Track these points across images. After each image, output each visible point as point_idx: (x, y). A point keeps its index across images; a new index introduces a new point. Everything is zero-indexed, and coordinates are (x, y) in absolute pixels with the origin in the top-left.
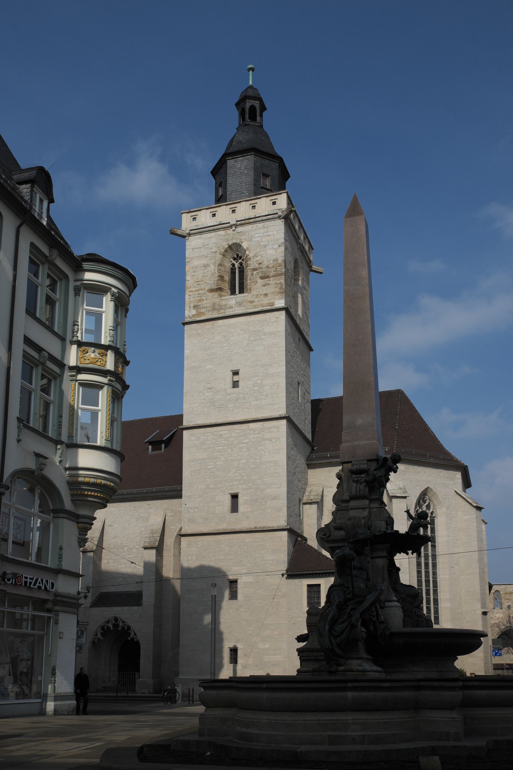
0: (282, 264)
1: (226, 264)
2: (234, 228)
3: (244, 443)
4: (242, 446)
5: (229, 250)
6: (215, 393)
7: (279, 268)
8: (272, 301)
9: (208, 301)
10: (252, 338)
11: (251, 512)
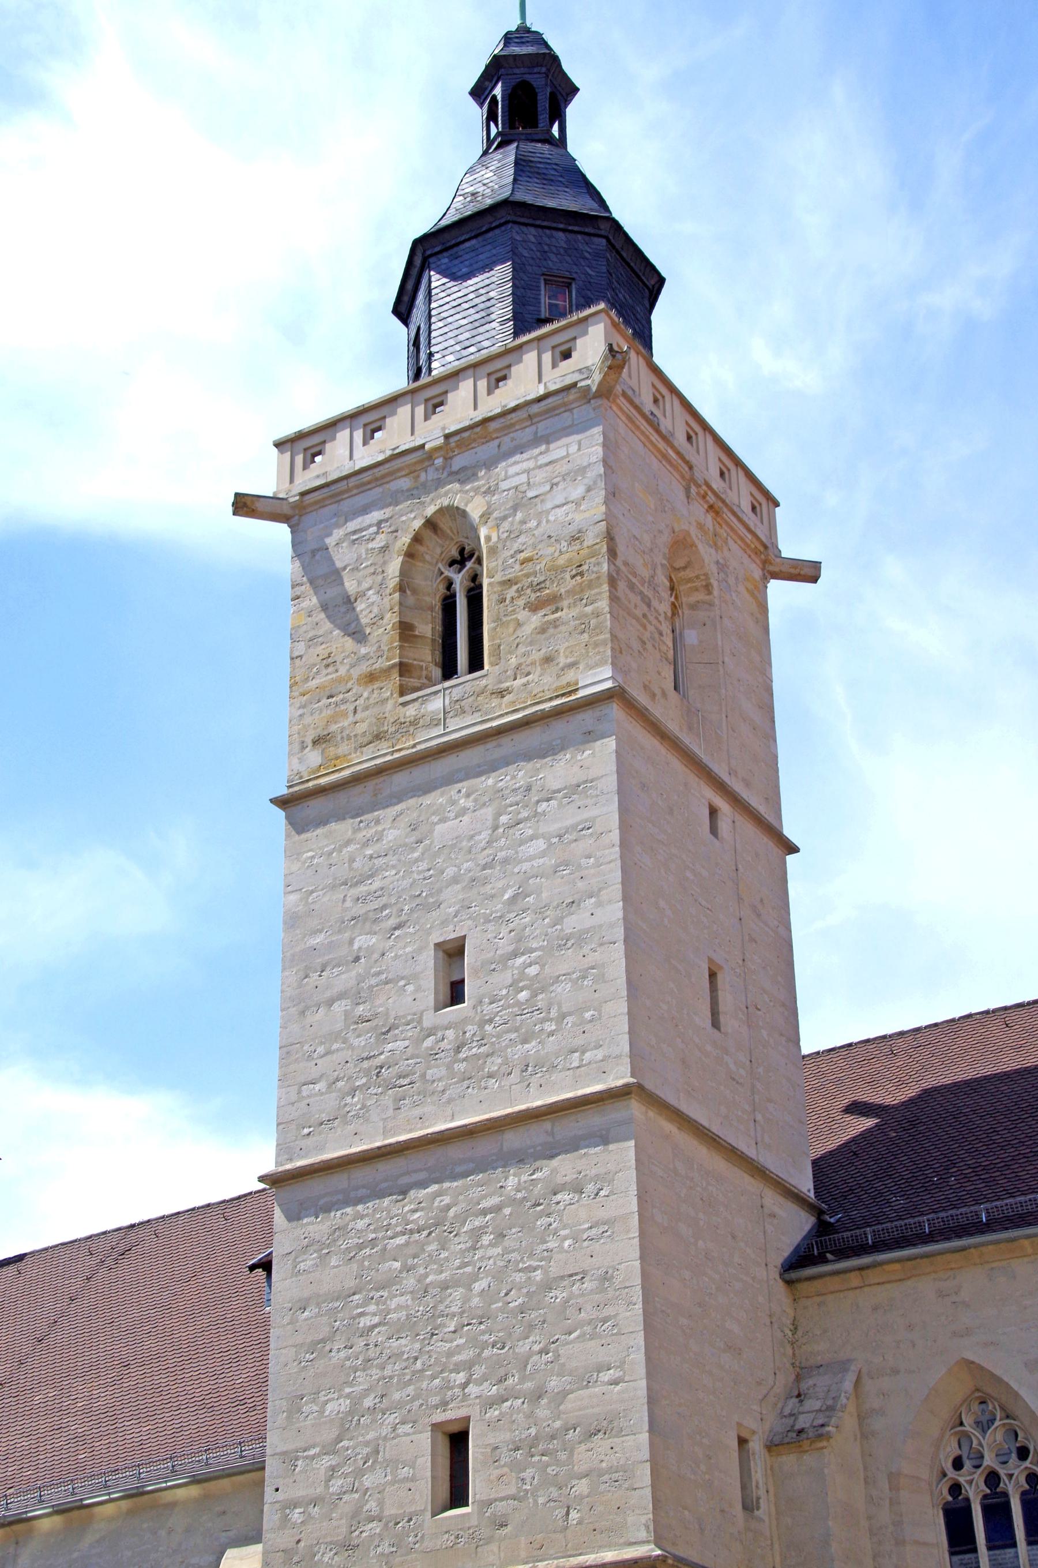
0: (600, 549)
1: (423, 583)
2: (439, 462)
3: (484, 1212)
4: (478, 1222)
5: (428, 534)
6: (384, 1034)
7: (588, 561)
8: (570, 676)
9: (359, 716)
10: (504, 819)
11: (514, 1498)
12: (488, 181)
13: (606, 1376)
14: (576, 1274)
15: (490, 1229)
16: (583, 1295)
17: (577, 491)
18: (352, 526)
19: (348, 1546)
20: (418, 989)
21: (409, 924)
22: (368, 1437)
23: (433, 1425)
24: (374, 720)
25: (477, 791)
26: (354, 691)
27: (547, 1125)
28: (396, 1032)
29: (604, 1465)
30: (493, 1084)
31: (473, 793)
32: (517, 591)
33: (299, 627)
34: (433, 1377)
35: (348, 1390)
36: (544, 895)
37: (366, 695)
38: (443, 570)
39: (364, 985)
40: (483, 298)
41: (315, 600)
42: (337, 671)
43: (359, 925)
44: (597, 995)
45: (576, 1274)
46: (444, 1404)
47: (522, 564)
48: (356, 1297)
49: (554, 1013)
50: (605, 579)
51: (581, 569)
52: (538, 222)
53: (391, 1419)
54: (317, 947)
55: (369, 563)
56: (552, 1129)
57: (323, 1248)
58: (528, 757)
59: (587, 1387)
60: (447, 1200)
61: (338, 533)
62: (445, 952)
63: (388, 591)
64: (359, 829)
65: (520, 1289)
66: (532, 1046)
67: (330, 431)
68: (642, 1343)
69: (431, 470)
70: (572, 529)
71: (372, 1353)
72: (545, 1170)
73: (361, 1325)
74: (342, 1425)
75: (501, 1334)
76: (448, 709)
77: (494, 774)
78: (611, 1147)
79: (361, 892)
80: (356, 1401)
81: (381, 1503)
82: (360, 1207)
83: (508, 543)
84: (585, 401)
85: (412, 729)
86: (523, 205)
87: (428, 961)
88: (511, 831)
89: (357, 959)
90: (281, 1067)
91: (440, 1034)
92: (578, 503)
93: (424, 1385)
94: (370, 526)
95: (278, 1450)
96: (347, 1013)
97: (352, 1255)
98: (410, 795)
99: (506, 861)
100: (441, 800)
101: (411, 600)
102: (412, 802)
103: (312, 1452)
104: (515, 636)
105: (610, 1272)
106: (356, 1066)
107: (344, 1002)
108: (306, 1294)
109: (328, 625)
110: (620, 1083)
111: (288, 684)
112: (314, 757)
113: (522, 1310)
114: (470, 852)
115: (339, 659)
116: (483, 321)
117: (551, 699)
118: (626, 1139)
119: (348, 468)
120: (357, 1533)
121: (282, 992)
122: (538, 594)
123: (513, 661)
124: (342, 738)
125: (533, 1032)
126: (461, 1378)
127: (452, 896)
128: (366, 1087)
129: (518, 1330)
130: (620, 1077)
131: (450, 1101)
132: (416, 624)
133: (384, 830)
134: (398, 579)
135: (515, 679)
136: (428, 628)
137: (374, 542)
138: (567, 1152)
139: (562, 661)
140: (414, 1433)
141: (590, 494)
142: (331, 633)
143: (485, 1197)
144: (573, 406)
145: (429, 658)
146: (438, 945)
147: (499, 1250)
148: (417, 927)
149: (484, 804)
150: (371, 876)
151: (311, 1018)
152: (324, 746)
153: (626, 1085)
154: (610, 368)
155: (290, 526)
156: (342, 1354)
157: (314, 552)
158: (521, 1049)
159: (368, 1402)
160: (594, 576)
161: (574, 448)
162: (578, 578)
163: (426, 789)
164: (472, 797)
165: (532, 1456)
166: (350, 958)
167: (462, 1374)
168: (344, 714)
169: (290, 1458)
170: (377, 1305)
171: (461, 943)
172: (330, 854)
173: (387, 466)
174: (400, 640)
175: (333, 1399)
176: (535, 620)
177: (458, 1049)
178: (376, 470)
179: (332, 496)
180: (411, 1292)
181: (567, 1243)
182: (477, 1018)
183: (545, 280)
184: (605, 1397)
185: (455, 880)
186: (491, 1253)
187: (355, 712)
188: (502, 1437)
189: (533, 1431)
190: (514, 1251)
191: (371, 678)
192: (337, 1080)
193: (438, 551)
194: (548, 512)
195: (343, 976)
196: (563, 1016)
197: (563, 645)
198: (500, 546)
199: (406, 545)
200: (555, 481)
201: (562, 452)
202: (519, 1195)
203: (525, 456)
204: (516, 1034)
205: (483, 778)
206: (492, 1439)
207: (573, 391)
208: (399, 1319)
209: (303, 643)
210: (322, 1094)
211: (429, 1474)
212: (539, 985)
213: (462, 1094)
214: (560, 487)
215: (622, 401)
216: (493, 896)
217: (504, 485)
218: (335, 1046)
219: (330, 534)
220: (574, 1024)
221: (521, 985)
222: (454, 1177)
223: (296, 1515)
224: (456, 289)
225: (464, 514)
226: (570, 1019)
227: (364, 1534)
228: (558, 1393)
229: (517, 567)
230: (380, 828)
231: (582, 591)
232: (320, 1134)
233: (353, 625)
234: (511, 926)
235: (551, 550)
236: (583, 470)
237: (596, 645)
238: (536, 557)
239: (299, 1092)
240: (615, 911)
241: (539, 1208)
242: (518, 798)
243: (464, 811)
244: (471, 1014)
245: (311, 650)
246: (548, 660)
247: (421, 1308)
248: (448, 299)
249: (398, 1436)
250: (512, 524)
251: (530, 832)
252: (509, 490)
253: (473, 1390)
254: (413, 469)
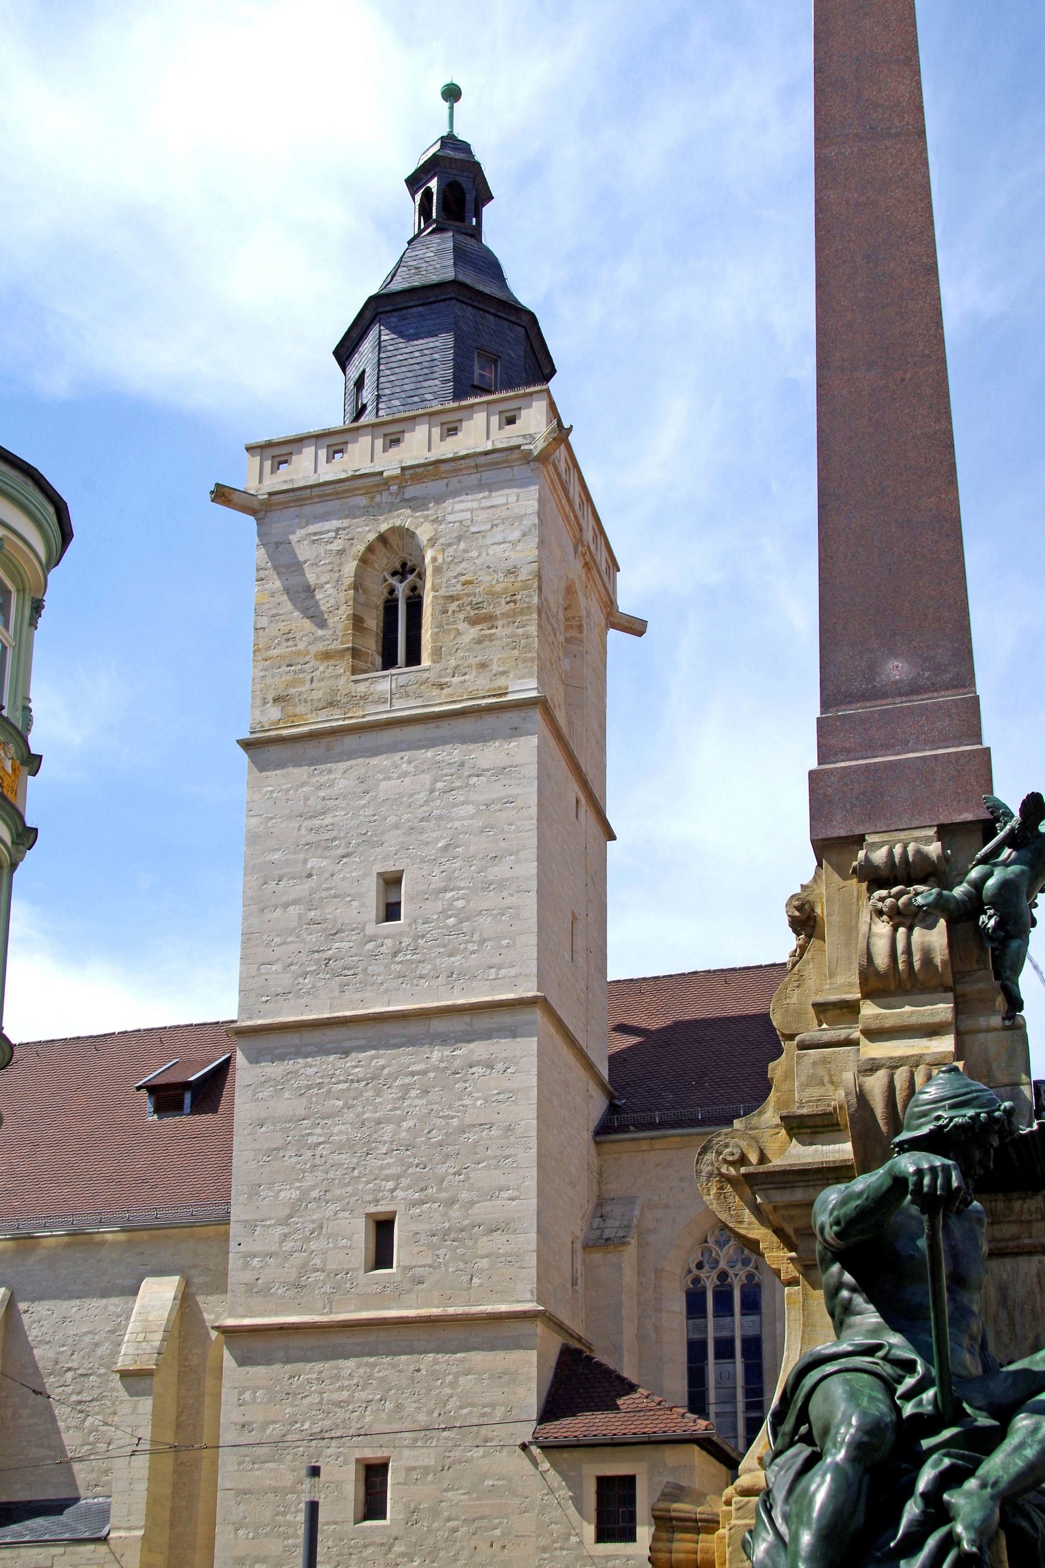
0: (532, 584)
1: (371, 586)
2: (394, 488)
3: (413, 1074)
4: (407, 1080)
5: (380, 546)
6: (332, 935)
7: (521, 593)
8: (501, 681)
12: (430, 259)
13: (506, 1194)
14: (486, 1124)
15: (417, 1086)
16: (490, 1139)
17: (516, 535)
18: (312, 528)
19: (298, 1285)
20: (362, 905)
21: (355, 855)
22: (314, 1217)
23: (367, 1214)
24: (329, 690)
25: (417, 760)
26: (311, 664)
27: (467, 1019)
28: (343, 934)
29: (501, 1251)
30: (424, 984)
31: (413, 761)
32: (459, 606)
33: (262, 604)
34: (368, 1183)
35: (298, 1184)
36: (472, 848)
37: (321, 668)
38: (387, 578)
39: (317, 896)
40: (427, 358)
41: (278, 584)
42: (296, 645)
43: (312, 849)
44: (512, 928)
45: (486, 1124)
46: (376, 1201)
47: (463, 585)
48: (305, 1122)
49: (476, 937)
50: (535, 609)
51: (514, 598)
52: (476, 304)
53: (332, 1207)
54: (275, 862)
55: (327, 561)
56: (471, 1021)
57: (279, 1086)
58: (464, 740)
59: (490, 1200)
60: (382, 1062)
61: (301, 533)
62: (384, 880)
63: (344, 587)
64: (314, 775)
65: (440, 1130)
66: (456, 960)
67: (296, 446)
68: (535, 1175)
69: (385, 494)
70: (509, 564)
71: (317, 1161)
72: (464, 1050)
73: (309, 1141)
74: (293, 1207)
75: (423, 1159)
76: (394, 691)
77: (433, 749)
78: (518, 1040)
79: (314, 825)
80: (305, 1193)
81: (324, 1261)
82: (309, 1060)
83: (452, 566)
84: (525, 462)
85: (362, 703)
86: (465, 286)
88: (446, 795)
89: (310, 876)
90: (243, 949)
91: (380, 941)
92: (514, 544)
93: (361, 1187)
94: (329, 531)
95: (241, 1219)
96: (300, 916)
97: (302, 1092)
98: (358, 755)
99: (440, 818)
100: (386, 762)
101: (362, 598)
102: (360, 760)
103: (268, 1223)
104: (455, 642)
105: (513, 1125)
106: (307, 956)
107: (298, 907)
108: (263, 1115)
109: (289, 606)
110: (530, 994)
111: (252, 649)
112: (274, 713)
113: (441, 1144)
114: (410, 806)
115: (298, 635)
116: (426, 377)
117: (484, 697)
118: (531, 1035)
119: (312, 480)
120: (305, 1278)
121: (244, 892)
122: (477, 612)
123: (453, 662)
124: (300, 700)
125: (459, 949)
126: (391, 1185)
127: (393, 840)
128: (317, 972)
129: (438, 1158)
130: (529, 990)
131: (386, 991)
132: (366, 618)
133: (336, 779)
134: (353, 579)
135: (453, 677)
136: (374, 622)
137: (332, 545)
138: (482, 1039)
139: (495, 668)
140: (352, 1218)
141: (525, 538)
142: (292, 613)
143: (414, 1063)
144: (514, 464)
145: (374, 648)
146: (380, 875)
147: (424, 1101)
148: (362, 858)
149: (423, 771)
150: (324, 813)
151: (268, 915)
152: (283, 704)
153: (535, 997)
154: (554, 439)
155: (256, 519)
156: (294, 1160)
157: (277, 544)
158: (447, 961)
159: (314, 1194)
160: (526, 605)
161: (513, 499)
162: (512, 604)
163: (374, 752)
164: (413, 764)
165: (445, 1241)
166: (304, 874)
167: (391, 1183)
168: (302, 682)
169: (251, 1226)
170: (323, 1129)
171: (399, 875)
172: (288, 791)
173: (348, 483)
174: (353, 629)
175: (286, 1189)
176: (473, 632)
177: (395, 954)
178: (337, 486)
179: (295, 501)
180: (351, 1123)
181: (479, 1103)
182: (412, 933)
183: (478, 353)
184: (504, 1208)
185: (396, 826)
186: (416, 1103)
187: (312, 681)
188: (422, 1227)
189: (447, 1225)
190: (436, 1103)
191: (326, 656)
192: (292, 964)
193: (385, 561)
194: (488, 547)
195: (298, 887)
196: (483, 941)
197: (495, 655)
198: (445, 567)
199: (361, 552)
200: (496, 522)
201: (503, 500)
202: (442, 1065)
203: (470, 497)
204: (444, 949)
205: (423, 751)
206: (415, 1227)
207: (517, 451)
208: (341, 1141)
209: (266, 618)
210: (278, 973)
211: (363, 1245)
212: (464, 917)
213: (397, 987)
214: (499, 529)
215: (551, 468)
216: (428, 843)
217: (450, 518)
218: (290, 939)
219: (294, 533)
220: (492, 948)
221: (449, 913)
222: (389, 1047)
223: (256, 1262)
224: (402, 345)
225: (412, 535)
226: (489, 944)
227: (310, 1279)
228: (468, 1202)
229: (459, 587)
230: (332, 777)
231: (515, 615)
232: (276, 1002)
233: (312, 610)
234: (443, 868)
235: (488, 578)
236: (520, 518)
237: (525, 660)
238: (476, 581)
239: (259, 969)
240: (530, 869)
241: (457, 1076)
242: (453, 771)
243: (406, 774)
244: (407, 929)
245: (273, 624)
246: (483, 666)
247: (359, 1135)
248: (395, 353)
249: (338, 1218)
250: (456, 551)
251: (462, 798)
252: (455, 522)
253: (399, 1193)
254: (370, 490)
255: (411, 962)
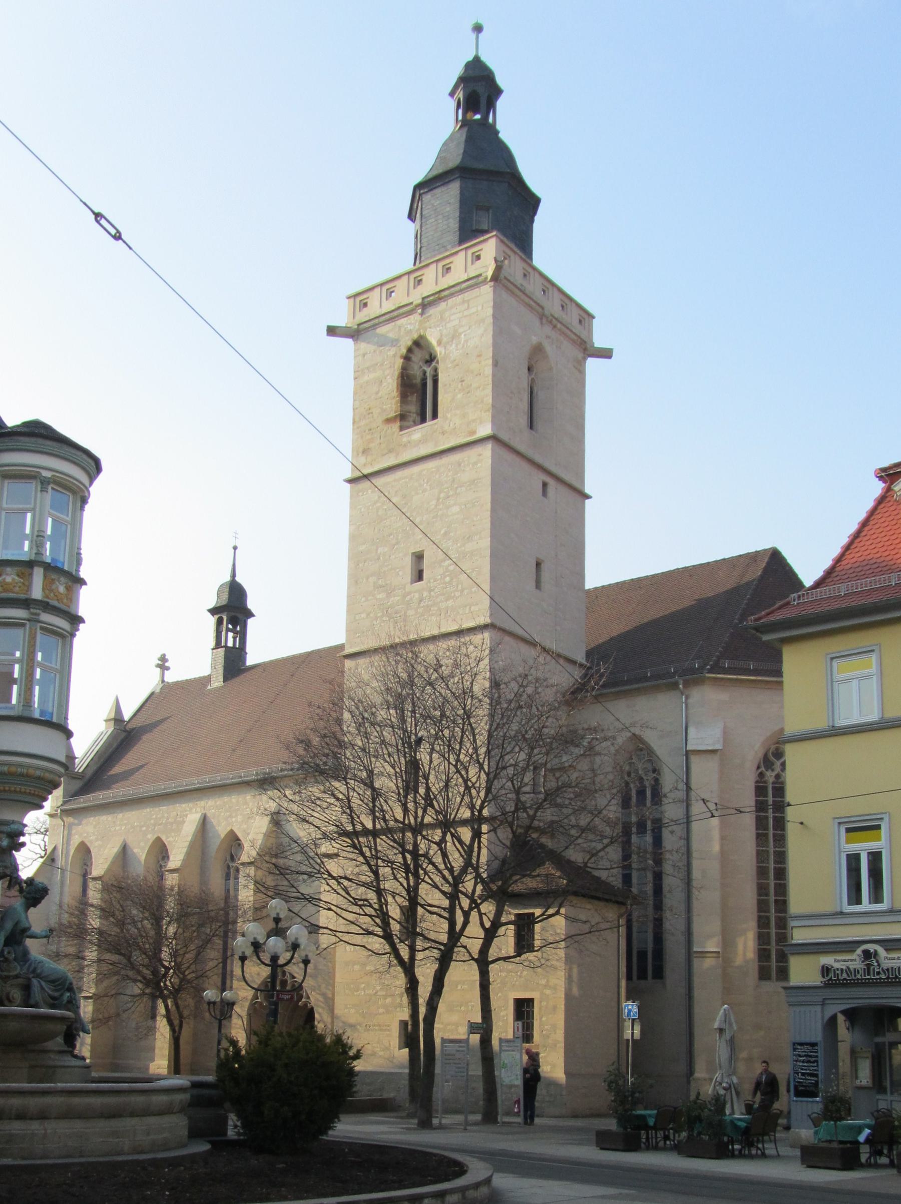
10: (442, 495)
87: (408, 561)
146: (413, 554)
255: (428, 606)
